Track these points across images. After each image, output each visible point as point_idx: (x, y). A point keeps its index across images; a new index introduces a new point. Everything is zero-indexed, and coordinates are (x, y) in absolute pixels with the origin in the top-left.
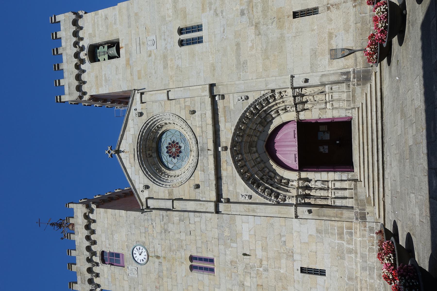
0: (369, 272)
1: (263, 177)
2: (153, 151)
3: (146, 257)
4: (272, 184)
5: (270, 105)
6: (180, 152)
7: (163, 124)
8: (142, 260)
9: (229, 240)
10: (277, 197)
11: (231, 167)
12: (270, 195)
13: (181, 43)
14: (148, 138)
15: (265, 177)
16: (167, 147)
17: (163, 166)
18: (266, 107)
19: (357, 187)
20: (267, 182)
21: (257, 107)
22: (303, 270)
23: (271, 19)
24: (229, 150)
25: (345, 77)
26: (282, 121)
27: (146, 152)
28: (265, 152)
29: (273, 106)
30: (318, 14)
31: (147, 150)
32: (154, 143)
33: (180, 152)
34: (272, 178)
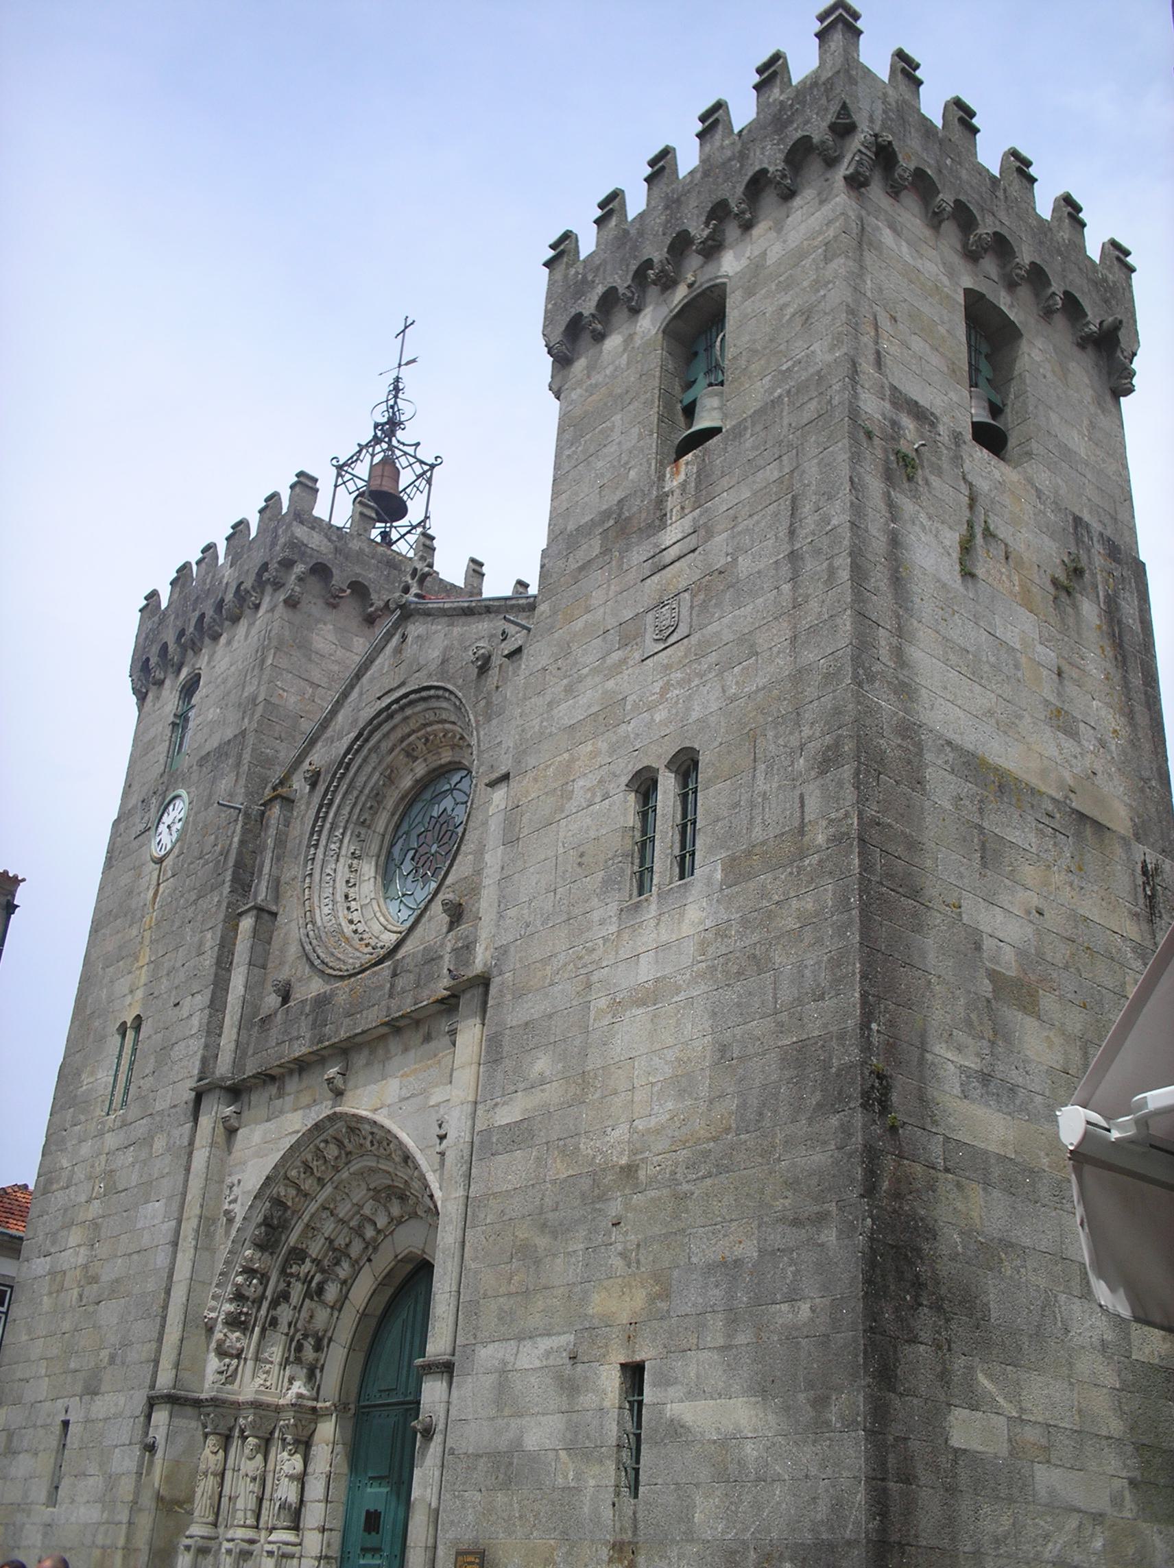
1: (308, 1260)
2: (430, 758)
10: (234, 1322)
11: (297, 1128)
12: (239, 1297)
13: (645, 785)
14: (447, 726)
15: (307, 1266)
17: (396, 817)
23: (638, 1245)
27: (414, 732)
30: (618, 1494)
31: (419, 734)
32: (450, 753)
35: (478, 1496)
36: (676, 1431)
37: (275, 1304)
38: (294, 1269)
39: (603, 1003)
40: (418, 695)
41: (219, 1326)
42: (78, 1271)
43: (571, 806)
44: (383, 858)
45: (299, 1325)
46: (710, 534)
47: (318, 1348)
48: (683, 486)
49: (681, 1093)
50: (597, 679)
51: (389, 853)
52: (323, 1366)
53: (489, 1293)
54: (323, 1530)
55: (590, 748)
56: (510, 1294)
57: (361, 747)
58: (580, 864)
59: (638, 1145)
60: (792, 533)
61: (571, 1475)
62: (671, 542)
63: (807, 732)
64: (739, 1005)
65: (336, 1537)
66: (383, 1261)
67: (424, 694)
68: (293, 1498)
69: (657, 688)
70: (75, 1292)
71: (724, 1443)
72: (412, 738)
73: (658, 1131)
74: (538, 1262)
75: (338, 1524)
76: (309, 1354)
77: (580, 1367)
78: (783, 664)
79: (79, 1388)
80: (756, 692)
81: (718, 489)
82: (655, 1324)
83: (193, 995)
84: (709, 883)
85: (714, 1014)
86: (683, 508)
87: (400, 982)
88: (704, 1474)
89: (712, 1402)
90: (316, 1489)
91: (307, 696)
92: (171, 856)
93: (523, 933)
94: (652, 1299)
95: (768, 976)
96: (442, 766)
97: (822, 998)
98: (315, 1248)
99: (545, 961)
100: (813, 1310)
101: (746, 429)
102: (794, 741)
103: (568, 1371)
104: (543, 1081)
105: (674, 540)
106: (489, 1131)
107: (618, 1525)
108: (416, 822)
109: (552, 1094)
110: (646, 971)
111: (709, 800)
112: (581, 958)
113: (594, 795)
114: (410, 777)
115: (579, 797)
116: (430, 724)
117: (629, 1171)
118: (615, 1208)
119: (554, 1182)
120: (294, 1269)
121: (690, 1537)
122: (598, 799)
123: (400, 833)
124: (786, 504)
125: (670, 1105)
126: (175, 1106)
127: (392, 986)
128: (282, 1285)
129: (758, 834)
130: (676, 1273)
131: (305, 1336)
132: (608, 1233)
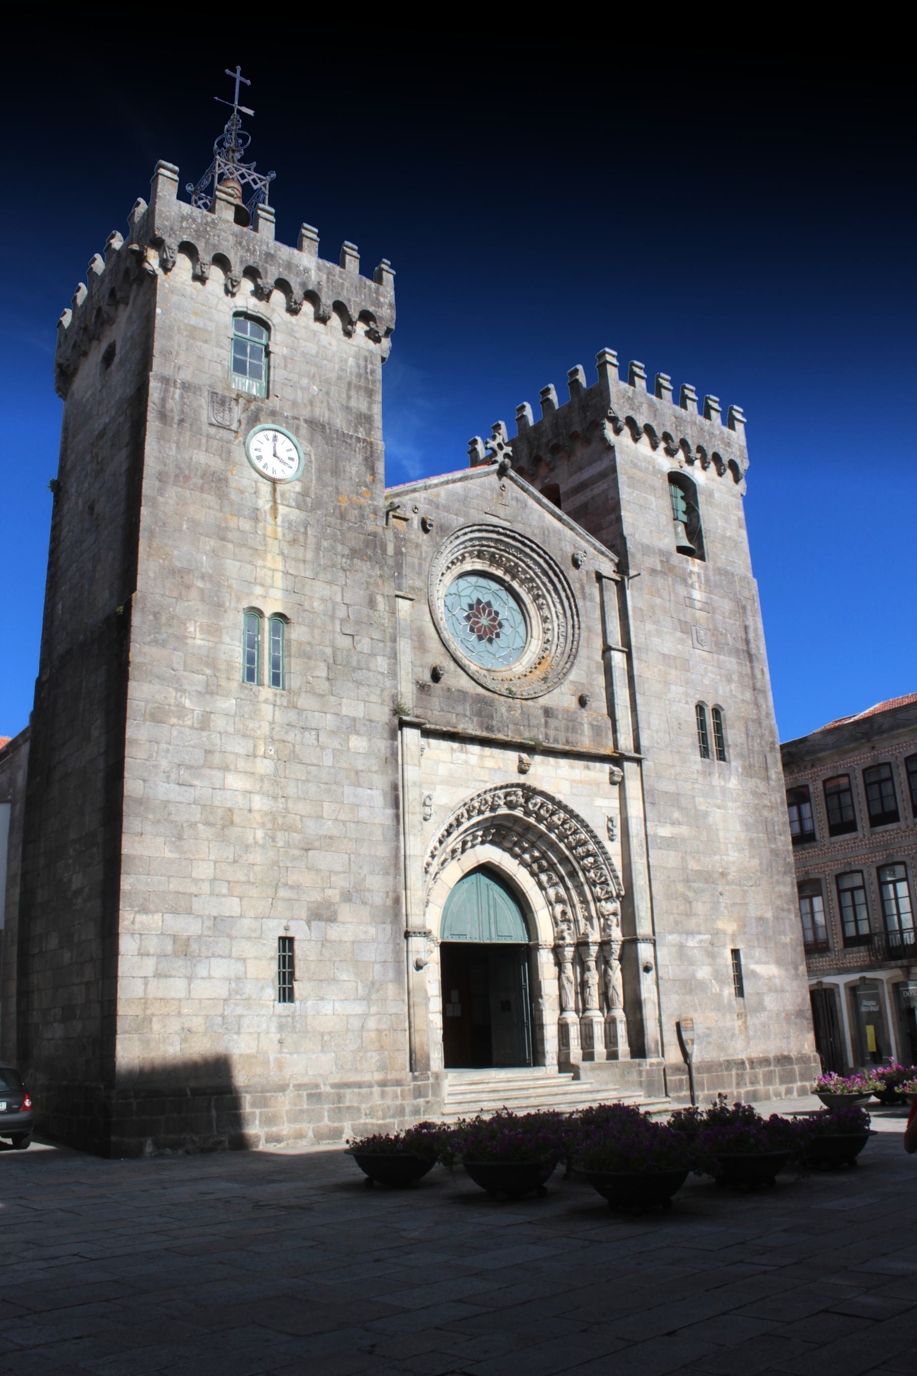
0: (308, 1110)
5: (586, 888)
7: (546, 612)
9: (339, 747)
16: (489, 604)
18: (582, 879)
21: (591, 859)
22: (287, 943)
24: (522, 779)
29: (581, 894)
35: (677, 997)
36: (754, 974)
42: (258, 817)
56: (679, 914)
70: (260, 834)
71: (770, 979)
73: (733, 863)
74: (690, 903)
77: (716, 949)
79: (304, 914)
83: (372, 639)
84: (737, 770)
85: (746, 825)
88: (765, 989)
94: (738, 925)
97: (780, 835)
103: (710, 949)
104: (679, 823)
109: (684, 830)
117: (722, 874)
119: (692, 870)
126: (371, 721)
127: (546, 723)
132: (718, 897)
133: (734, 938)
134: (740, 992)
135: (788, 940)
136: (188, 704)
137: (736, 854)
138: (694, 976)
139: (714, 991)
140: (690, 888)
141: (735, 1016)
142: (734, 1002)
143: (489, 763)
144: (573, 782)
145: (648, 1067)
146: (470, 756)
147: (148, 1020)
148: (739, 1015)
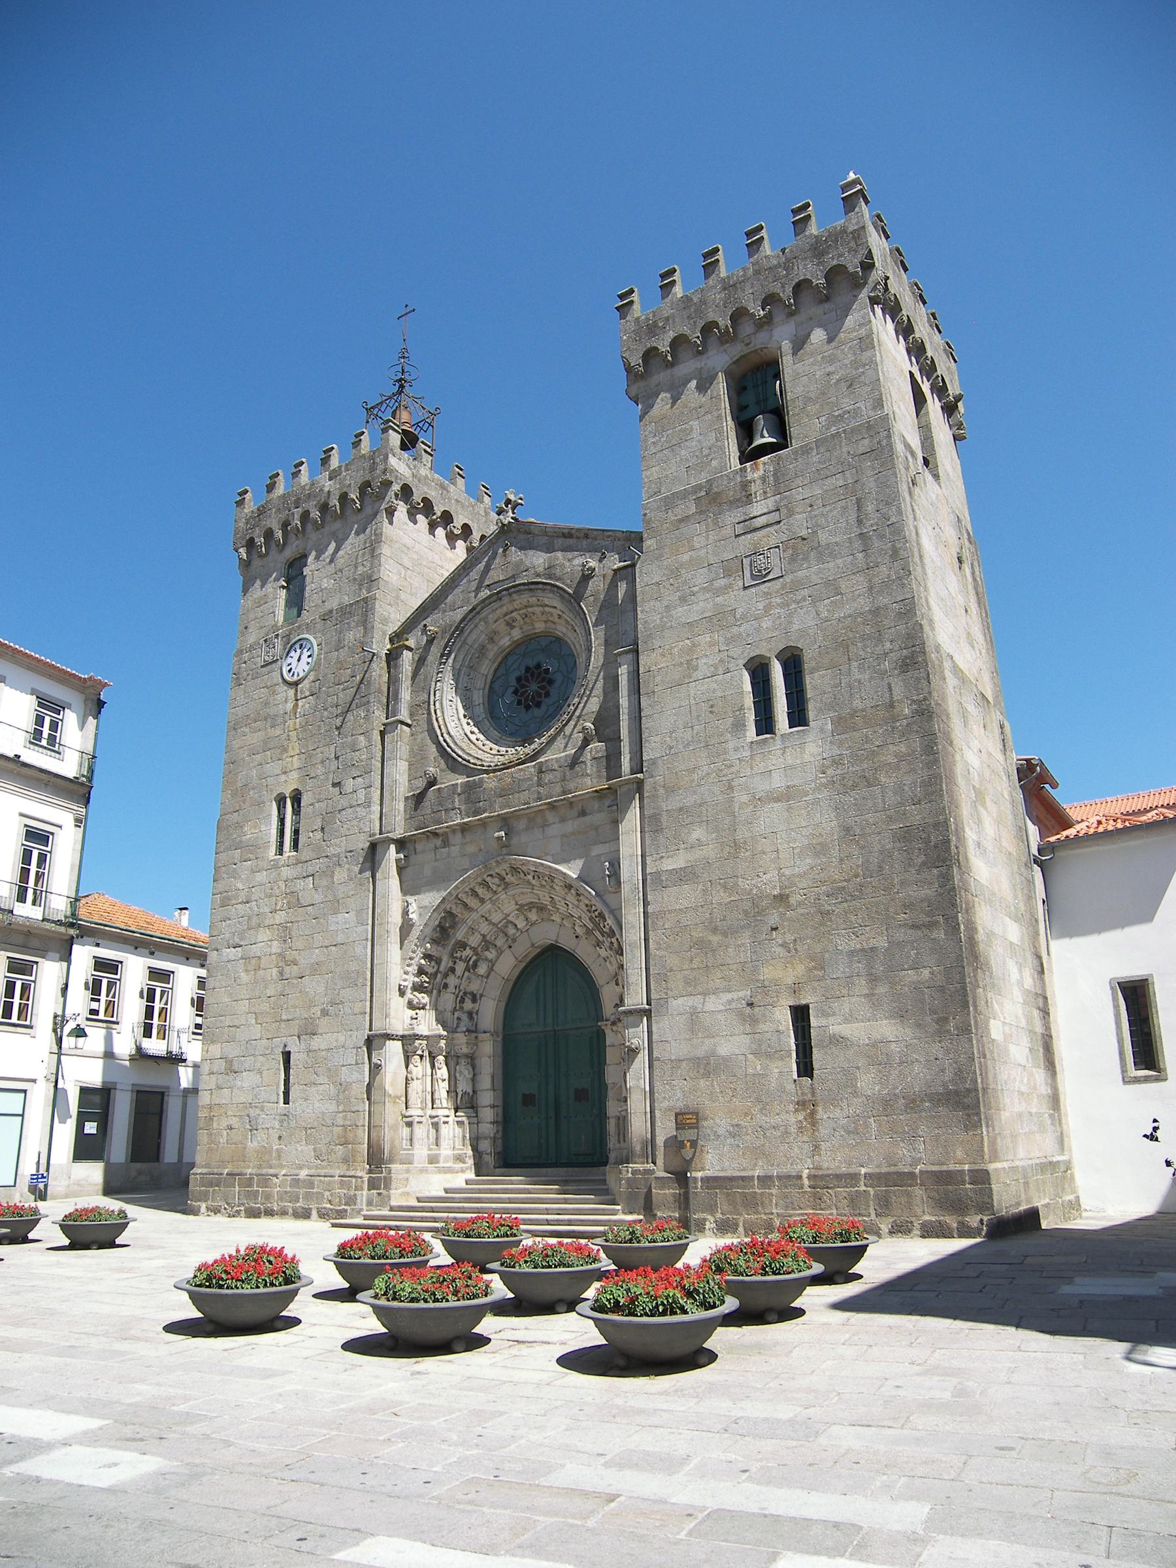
1: (468, 948)
3: (295, 678)
4: (456, 972)
6: (528, 708)
8: (291, 669)
14: (547, 609)
17: (496, 664)
19: (445, 1173)
20: (458, 961)
25: (638, 1148)
26: (601, 984)
27: (516, 610)
28: (533, 945)
31: (521, 612)
33: (528, 708)
34: (474, 970)
36: (837, 1041)
37: (446, 975)
38: (458, 955)
39: (745, 798)
40: (526, 587)
41: (409, 991)
43: (699, 674)
44: (487, 691)
45: (462, 988)
46: (791, 513)
47: (474, 1000)
48: (763, 479)
49: (817, 854)
50: (708, 596)
51: (491, 688)
52: (478, 1011)
53: (674, 968)
54: (493, 1106)
55: (708, 639)
57: (474, 617)
58: (711, 712)
59: (786, 883)
60: (860, 522)
61: (759, 1067)
62: (759, 513)
63: (888, 645)
64: (855, 805)
65: (500, 1110)
66: (524, 948)
67: (533, 587)
68: (470, 1090)
69: (761, 606)
71: (874, 1045)
72: (514, 614)
75: (500, 1102)
76: (468, 1005)
77: (757, 1009)
78: (864, 604)
80: (845, 617)
81: (794, 485)
82: (816, 984)
83: (354, 778)
84: (822, 730)
86: (765, 493)
87: (547, 778)
89: (863, 1024)
90: (485, 1082)
91: (402, 576)
92: (306, 681)
93: (668, 752)
94: (810, 970)
95: (877, 790)
96: (535, 633)
97: (919, 802)
98: (474, 940)
99: (691, 771)
100: (932, 973)
101: (811, 449)
102: (879, 650)
105: (762, 512)
106: (658, 873)
107: (799, 1092)
108: (512, 669)
109: (709, 852)
110: (778, 782)
111: (811, 682)
112: (721, 770)
113: (716, 668)
114: (508, 638)
115: (703, 669)
116: (532, 607)
117: (782, 899)
118: (773, 918)
120: (458, 955)
121: (855, 1094)
122: (720, 672)
123: (499, 674)
124: (851, 503)
125: (808, 861)
126: (351, 851)
127: (539, 779)
128: (451, 964)
129: (857, 704)
130: (827, 955)
131: (465, 993)
133: (795, 990)
134: (806, 1068)
135: (926, 973)
136: (240, 886)
137: (808, 861)
138: (713, 1053)
139: (750, 1071)
140: (715, 930)
141: (791, 1107)
142: (791, 1087)
143: (471, 849)
144: (564, 836)
145: (630, 1175)
146: (452, 848)
147: (211, 1119)
148: (801, 1104)
